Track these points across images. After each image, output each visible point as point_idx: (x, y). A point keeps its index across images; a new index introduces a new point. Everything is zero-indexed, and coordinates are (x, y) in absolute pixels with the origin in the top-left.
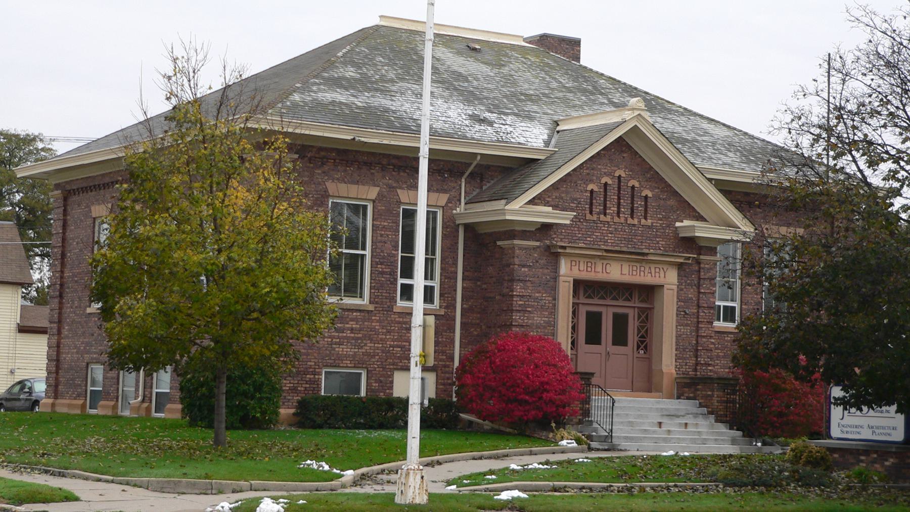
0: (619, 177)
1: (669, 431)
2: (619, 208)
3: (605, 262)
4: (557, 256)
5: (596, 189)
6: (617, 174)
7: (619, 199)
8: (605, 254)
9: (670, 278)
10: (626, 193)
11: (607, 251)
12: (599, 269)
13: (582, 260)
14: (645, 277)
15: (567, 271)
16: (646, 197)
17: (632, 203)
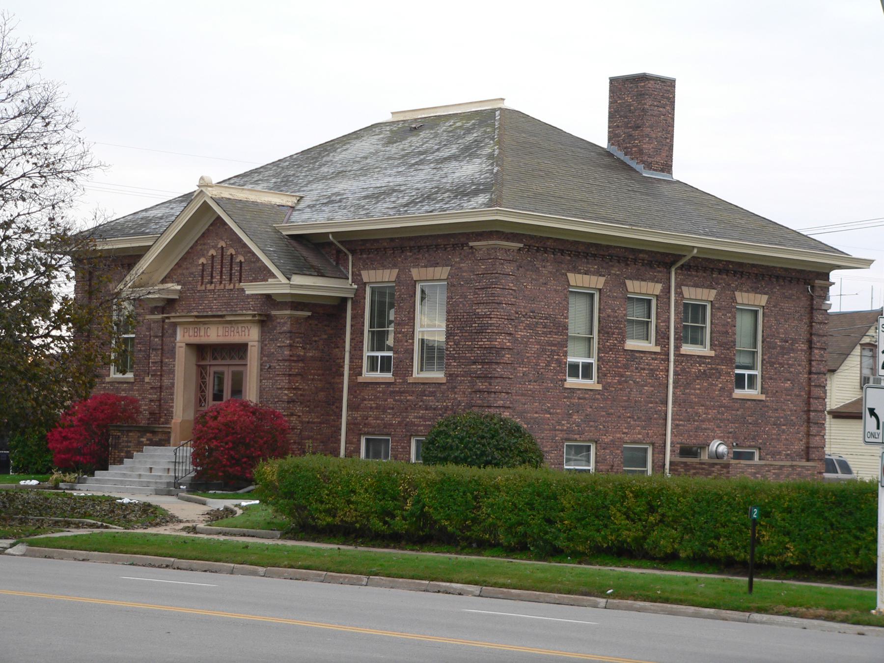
0: (222, 248)
1: (140, 475)
2: (221, 276)
3: (206, 326)
4: (175, 325)
5: (205, 262)
6: (219, 246)
7: (222, 268)
8: (196, 320)
9: (251, 335)
10: (227, 261)
11: (197, 317)
12: (202, 333)
13: (191, 327)
14: (234, 336)
15: (182, 337)
16: (241, 262)
17: (231, 270)
